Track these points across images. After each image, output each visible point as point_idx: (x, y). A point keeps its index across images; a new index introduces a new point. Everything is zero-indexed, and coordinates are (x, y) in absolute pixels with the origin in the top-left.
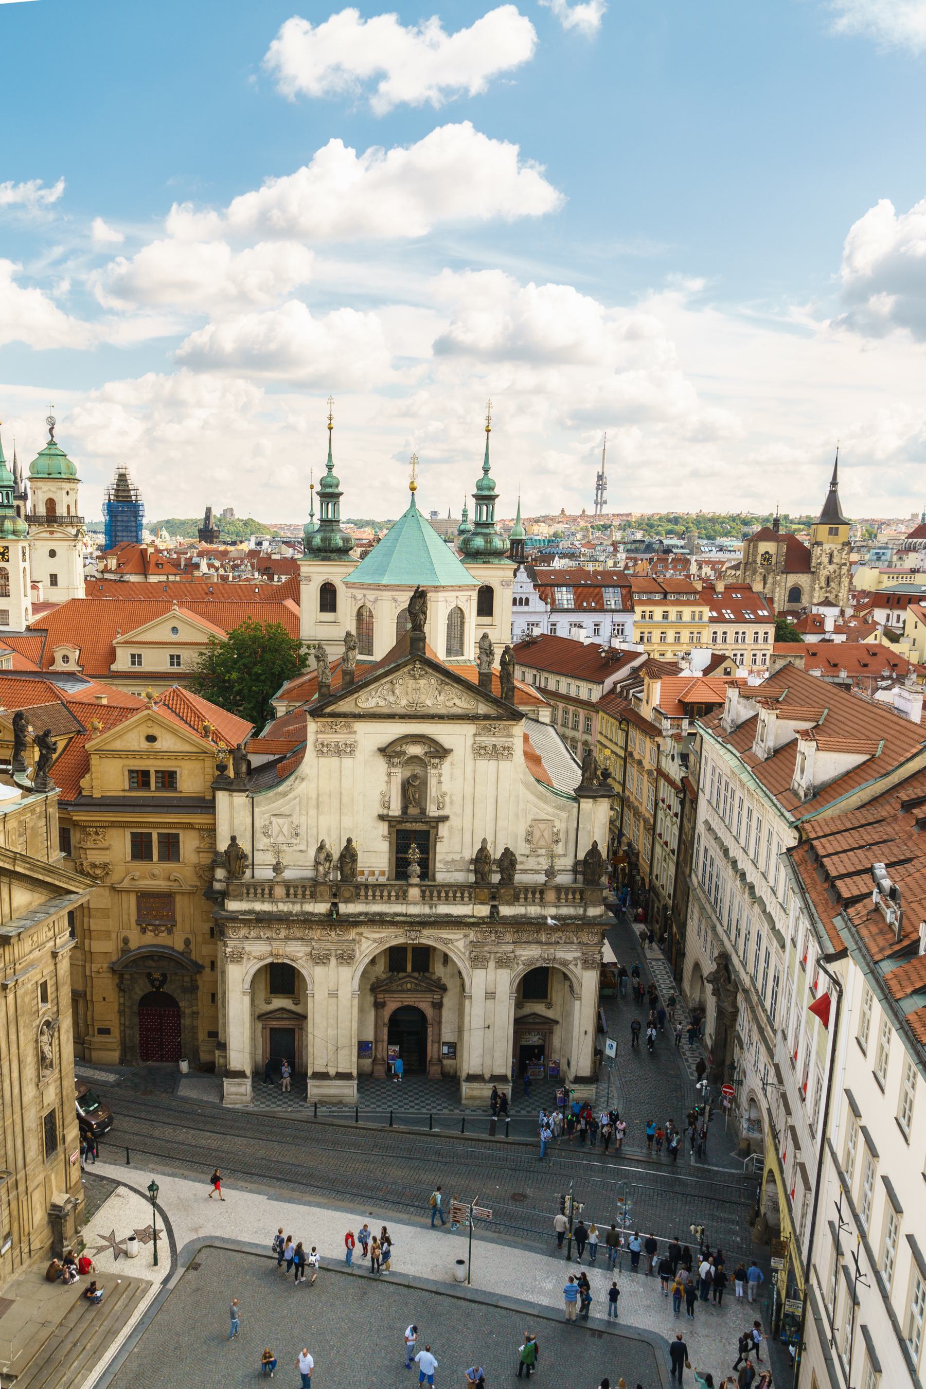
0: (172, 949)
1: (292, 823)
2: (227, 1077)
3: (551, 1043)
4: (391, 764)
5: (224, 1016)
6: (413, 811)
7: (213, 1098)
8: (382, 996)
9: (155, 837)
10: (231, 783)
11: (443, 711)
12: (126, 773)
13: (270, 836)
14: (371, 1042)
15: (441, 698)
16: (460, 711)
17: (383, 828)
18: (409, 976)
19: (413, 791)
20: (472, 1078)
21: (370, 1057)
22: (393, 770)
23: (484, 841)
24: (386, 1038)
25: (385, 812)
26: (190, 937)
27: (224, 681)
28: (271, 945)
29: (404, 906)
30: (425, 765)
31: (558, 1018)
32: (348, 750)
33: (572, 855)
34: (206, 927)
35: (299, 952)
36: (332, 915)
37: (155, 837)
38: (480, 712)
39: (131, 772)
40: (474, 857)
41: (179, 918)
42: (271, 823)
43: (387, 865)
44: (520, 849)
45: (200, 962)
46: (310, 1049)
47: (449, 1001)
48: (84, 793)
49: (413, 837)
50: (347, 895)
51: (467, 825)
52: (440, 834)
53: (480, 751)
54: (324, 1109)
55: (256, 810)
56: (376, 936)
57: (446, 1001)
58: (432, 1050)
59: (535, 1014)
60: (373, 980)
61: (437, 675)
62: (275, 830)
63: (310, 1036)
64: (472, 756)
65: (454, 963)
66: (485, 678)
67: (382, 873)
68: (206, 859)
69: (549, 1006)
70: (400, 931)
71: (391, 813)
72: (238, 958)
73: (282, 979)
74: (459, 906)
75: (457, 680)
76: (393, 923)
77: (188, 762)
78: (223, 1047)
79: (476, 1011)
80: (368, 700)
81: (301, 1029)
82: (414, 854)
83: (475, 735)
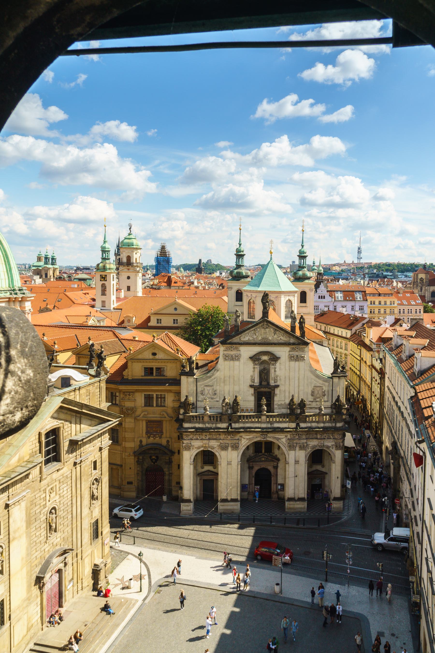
0: (161, 445)
1: (213, 389)
2: (182, 502)
4: (255, 364)
6: (264, 383)
7: (176, 512)
9: (155, 396)
10: (187, 372)
11: (276, 342)
12: (143, 369)
14: (247, 485)
15: (276, 336)
16: (283, 342)
17: (252, 391)
18: (263, 455)
19: (264, 374)
22: (256, 366)
23: (293, 396)
24: (254, 482)
25: (253, 384)
26: (169, 440)
30: (269, 364)
32: (237, 358)
34: (176, 435)
37: (155, 396)
38: (291, 342)
39: (145, 368)
42: (204, 389)
43: (253, 406)
44: (308, 399)
45: (173, 450)
46: (219, 489)
48: (125, 377)
51: (287, 389)
52: (276, 393)
53: (292, 358)
54: (225, 516)
55: (198, 384)
60: (248, 456)
61: (273, 327)
62: (206, 392)
63: (219, 483)
64: (288, 360)
65: (282, 449)
66: (293, 328)
68: (177, 405)
70: (258, 435)
71: (255, 384)
78: (181, 488)
79: (291, 469)
80: (246, 337)
82: (264, 401)
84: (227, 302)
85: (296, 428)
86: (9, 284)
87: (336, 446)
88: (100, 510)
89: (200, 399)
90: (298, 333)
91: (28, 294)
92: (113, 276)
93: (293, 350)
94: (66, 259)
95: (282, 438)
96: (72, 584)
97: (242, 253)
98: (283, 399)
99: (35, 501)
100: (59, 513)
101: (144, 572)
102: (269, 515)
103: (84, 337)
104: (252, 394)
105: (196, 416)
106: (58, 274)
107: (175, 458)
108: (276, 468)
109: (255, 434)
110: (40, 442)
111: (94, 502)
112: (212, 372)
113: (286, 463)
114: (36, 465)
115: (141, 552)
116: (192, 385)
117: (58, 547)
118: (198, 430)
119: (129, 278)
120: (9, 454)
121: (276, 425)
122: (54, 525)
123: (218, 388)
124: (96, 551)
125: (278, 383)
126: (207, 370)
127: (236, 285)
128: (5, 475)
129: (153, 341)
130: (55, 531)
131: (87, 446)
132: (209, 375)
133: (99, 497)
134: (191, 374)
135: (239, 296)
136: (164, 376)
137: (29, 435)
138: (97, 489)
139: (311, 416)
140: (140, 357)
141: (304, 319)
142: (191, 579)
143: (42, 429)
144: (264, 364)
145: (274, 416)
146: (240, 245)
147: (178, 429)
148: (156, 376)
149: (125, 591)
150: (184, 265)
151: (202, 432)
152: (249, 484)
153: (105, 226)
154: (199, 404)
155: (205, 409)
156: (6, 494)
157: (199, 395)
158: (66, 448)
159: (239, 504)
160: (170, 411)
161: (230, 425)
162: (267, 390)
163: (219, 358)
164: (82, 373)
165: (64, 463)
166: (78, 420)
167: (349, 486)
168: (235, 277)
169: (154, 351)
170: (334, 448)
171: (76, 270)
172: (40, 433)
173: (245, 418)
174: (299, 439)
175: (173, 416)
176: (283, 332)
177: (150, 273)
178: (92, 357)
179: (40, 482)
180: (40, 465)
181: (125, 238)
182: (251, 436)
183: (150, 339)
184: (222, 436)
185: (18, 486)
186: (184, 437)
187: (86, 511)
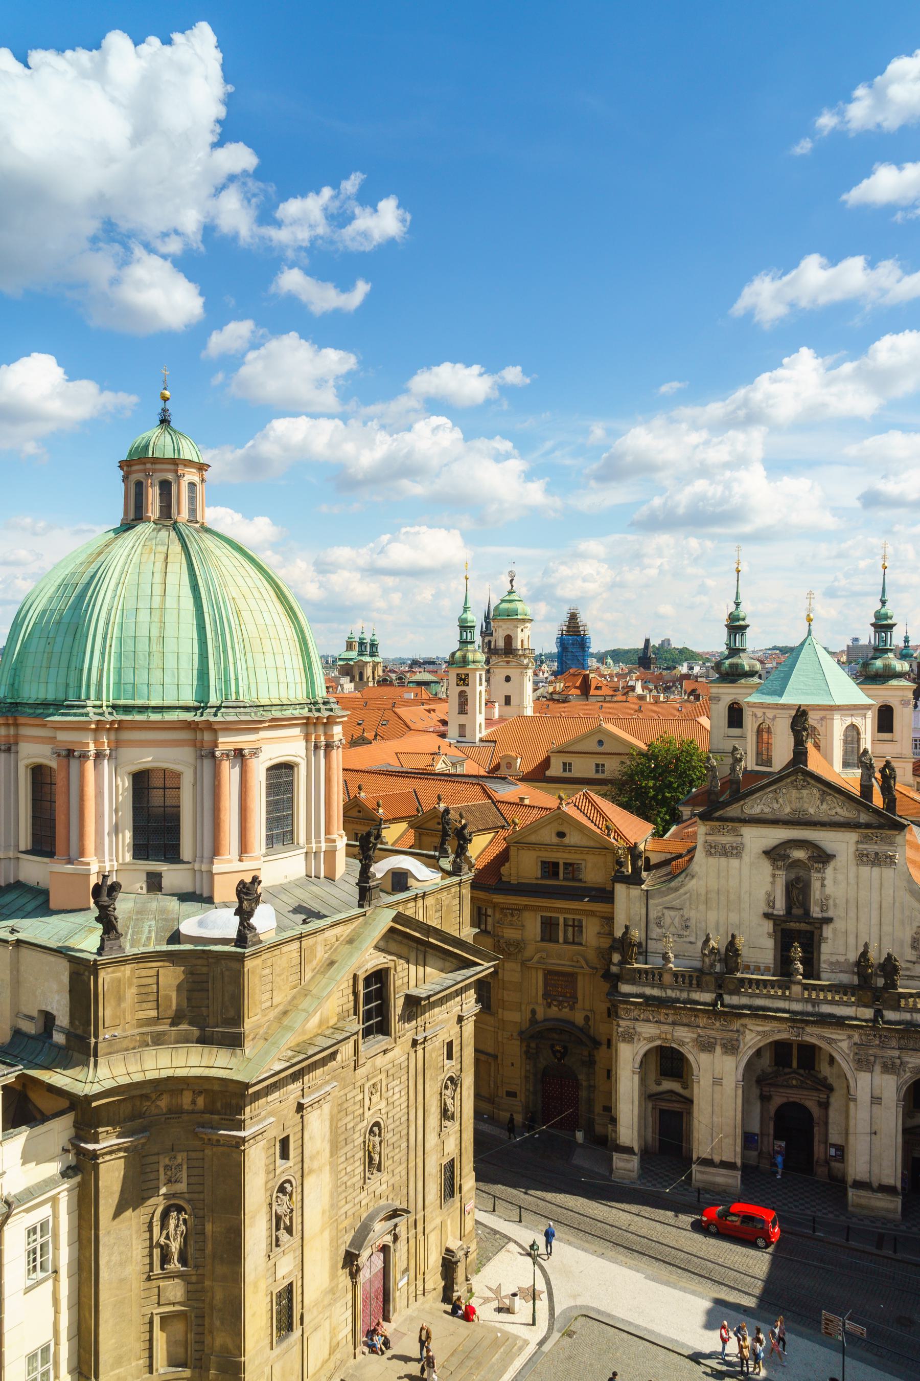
1: (683, 916)
6: (797, 911)
8: (767, 1089)
9: (561, 921)
11: (826, 819)
12: (539, 864)
14: (757, 1135)
15: (824, 806)
16: (842, 819)
17: (768, 926)
18: (794, 1072)
19: (798, 891)
20: (859, 1185)
21: (756, 1150)
22: (778, 872)
23: (866, 945)
24: (772, 1132)
25: (770, 911)
27: (642, 787)
28: (659, 1029)
32: (735, 852)
34: (603, 1007)
36: (717, 1005)
37: (561, 921)
38: (862, 821)
39: (543, 863)
41: (580, 997)
42: (663, 914)
43: (772, 961)
44: (905, 956)
46: (695, 1134)
47: (836, 1101)
48: (504, 879)
50: (732, 987)
51: (851, 927)
52: (824, 935)
53: (862, 858)
54: (708, 1196)
55: (651, 902)
56: (760, 1029)
57: (832, 1100)
58: (818, 1150)
61: (819, 786)
62: (668, 921)
63: (695, 1122)
64: (854, 862)
65: (839, 1065)
66: (866, 790)
67: (767, 969)
68: (606, 943)
70: (784, 1026)
71: (775, 912)
73: (669, 1063)
79: (861, 1116)
82: (797, 952)
83: (857, 842)
84: (709, 728)
85: (875, 1021)
86: (308, 693)
88: (456, 1141)
89: (653, 935)
90: (878, 800)
91: (338, 710)
92: (480, 675)
93: (866, 839)
94: (396, 647)
95: (841, 1041)
96: (405, 1280)
97: (742, 623)
98: (842, 950)
99: (345, 1106)
100: (387, 1136)
101: (541, 1286)
102: (808, 1212)
103: (430, 796)
104: (768, 934)
105: (646, 971)
106: (381, 673)
107: (601, 1054)
108: (825, 1106)
109: (775, 1024)
110: (355, 993)
111: (447, 1123)
112: (679, 879)
113: (850, 1098)
114: (348, 1037)
115: (534, 1242)
116: (637, 904)
117: (383, 1202)
118: (649, 1001)
119: (508, 679)
120: (304, 1010)
121: (826, 1009)
122: (376, 1157)
123: (693, 914)
124: (449, 1222)
125: (830, 914)
126: (670, 873)
127: (728, 693)
128: (297, 1049)
129: (559, 808)
130: (379, 1170)
131: (437, 1010)
132: (673, 884)
133: (457, 1115)
134: (635, 880)
135: (735, 715)
136: (580, 880)
137: (338, 978)
138: (453, 1098)
139: (911, 995)
140: (533, 838)
141: (892, 769)
142: (636, 1322)
143: (359, 968)
144: (798, 870)
145: (822, 988)
146: (738, 604)
147: (608, 994)
148: (565, 879)
149: (504, 1317)
150: (614, 651)
151: (658, 1007)
152: (762, 1133)
153: (467, 579)
154: (652, 946)
155: (665, 957)
156: (298, 1085)
157: (652, 926)
158: (399, 1011)
159: (738, 1174)
160: (591, 955)
161: (720, 997)
162: (803, 926)
163: (695, 848)
164: (428, 866)
165: (395, 1039)
166: (421, 957)
168: (727, 674)
169: (561, 829)
171: (411, 666)
172: (355, 975)
173: (754, 986)
174: (882, 1046)
175: (598, 966)
176: (842, 798)
177: (546, 669)
178: (445, 834)
179: (355, 1070)
180: (355, 1037)
181: (503, 601)
182: (767, 1027)
183: (552, 803)
184: (702, 1021)
185: (319, 1072)
186: (622, 1013)
187: (432, 1140)
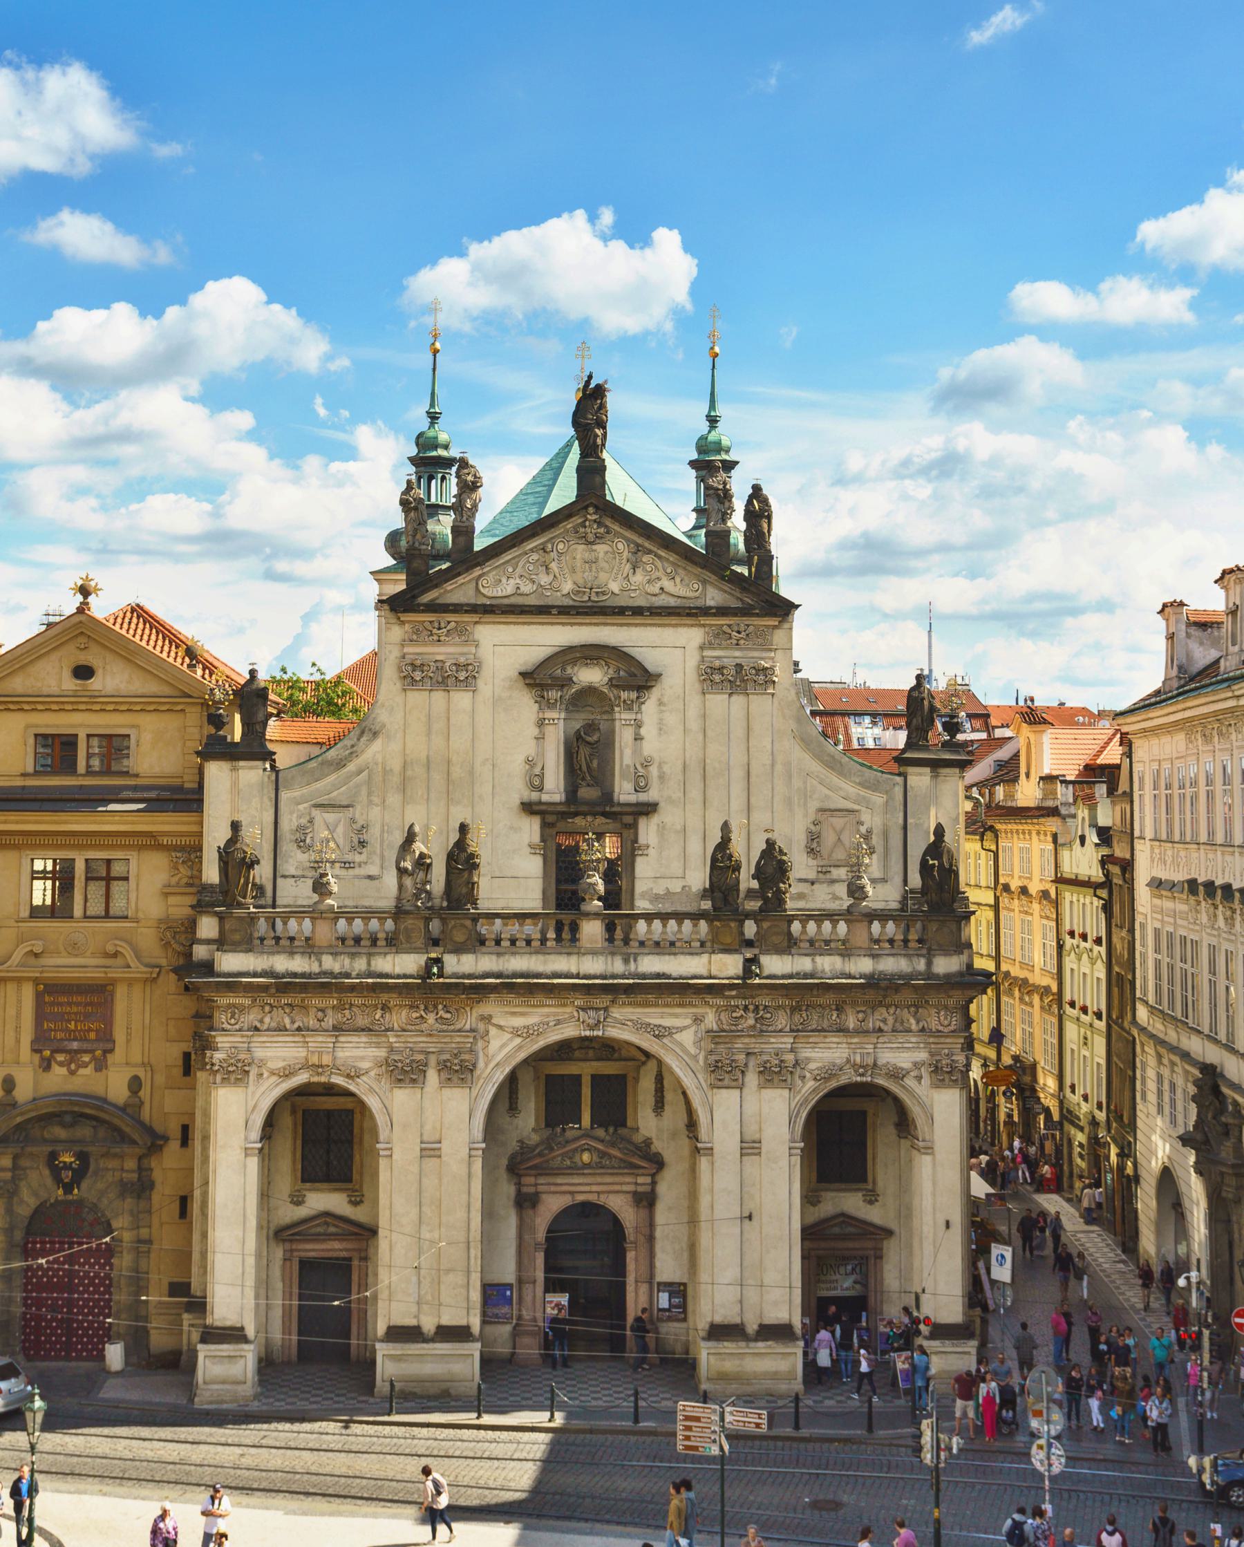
1: (353, 821)
3: (880, 1281)
4: (544, 703)
5: (204, 1235)
6: (586, 793)
8: (531, 1180)
11: (641, 602)
12: (31, 741)
13: (309, 847)
14: (510, 1286)
15: (639, 578)
16: (672, 602)
17: (531, 829)
18: (587, 1135)
19: (588, 755)
22: (550, 714)
23: (726, 827)
24: (540, 1275)
25: (535, 796)
26: (141, 1074)
29: (574, 959)
31: (892, 1225)
32: (462, 675)
33: (898, 879)
34: (174, 1052)
35: (362, 1058)
38: (710, 603)
40: (707, 886)
42: (311, 821)
45: (159, 1128)
47: (669, 1189)
49: (587, 808)
52: (642, 840)
53: (715, 678)
55: (284, 795)
56: (518, 1022)
57: (662, 1189)
58: (635, 1300)
59: (843, 1214)
60: (513, 1146)
61: (628, 534)
64: (697, 686)
69: (872, 1198)
71: (545, 798)
72: (238, 1073)
73: (323, 1135)
74: (681, 958)
75: (667, 542)
76: (550, 990)
77: (154, 716)
80: (500, 583)
81: (365, 1259)
83: (702, 648)
87: (936, 1069)
93: (719, 638)
116: (255, 802)
123: (375, 813)
125: (651, 795)
141: (764, 501)
148: (89, 773)
152: (520, 1281)
157: (287, 847)
160: (148, 939)
167: (1003, 1273)
170: (926, 1080)
174: (761, 1030)
175: (164, 962)
176: (672, 557)
